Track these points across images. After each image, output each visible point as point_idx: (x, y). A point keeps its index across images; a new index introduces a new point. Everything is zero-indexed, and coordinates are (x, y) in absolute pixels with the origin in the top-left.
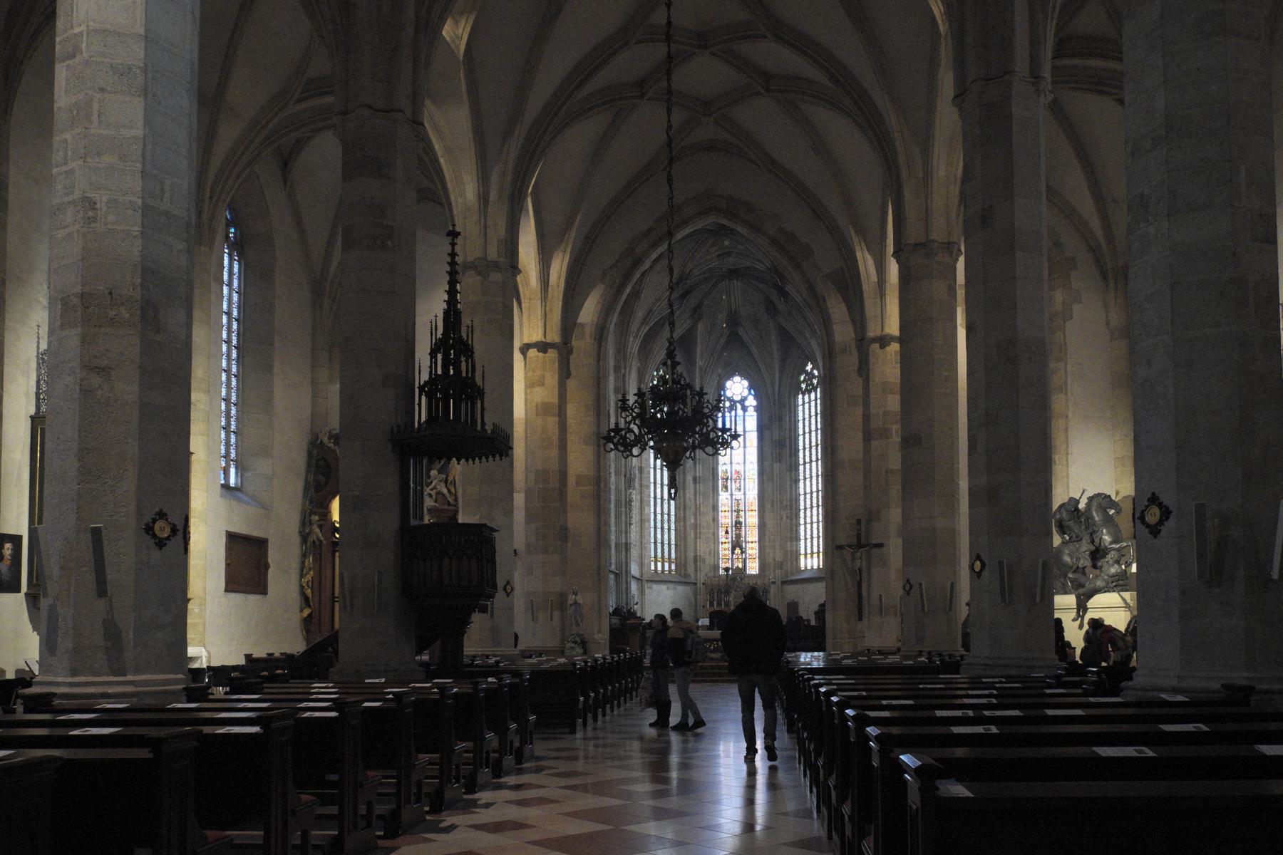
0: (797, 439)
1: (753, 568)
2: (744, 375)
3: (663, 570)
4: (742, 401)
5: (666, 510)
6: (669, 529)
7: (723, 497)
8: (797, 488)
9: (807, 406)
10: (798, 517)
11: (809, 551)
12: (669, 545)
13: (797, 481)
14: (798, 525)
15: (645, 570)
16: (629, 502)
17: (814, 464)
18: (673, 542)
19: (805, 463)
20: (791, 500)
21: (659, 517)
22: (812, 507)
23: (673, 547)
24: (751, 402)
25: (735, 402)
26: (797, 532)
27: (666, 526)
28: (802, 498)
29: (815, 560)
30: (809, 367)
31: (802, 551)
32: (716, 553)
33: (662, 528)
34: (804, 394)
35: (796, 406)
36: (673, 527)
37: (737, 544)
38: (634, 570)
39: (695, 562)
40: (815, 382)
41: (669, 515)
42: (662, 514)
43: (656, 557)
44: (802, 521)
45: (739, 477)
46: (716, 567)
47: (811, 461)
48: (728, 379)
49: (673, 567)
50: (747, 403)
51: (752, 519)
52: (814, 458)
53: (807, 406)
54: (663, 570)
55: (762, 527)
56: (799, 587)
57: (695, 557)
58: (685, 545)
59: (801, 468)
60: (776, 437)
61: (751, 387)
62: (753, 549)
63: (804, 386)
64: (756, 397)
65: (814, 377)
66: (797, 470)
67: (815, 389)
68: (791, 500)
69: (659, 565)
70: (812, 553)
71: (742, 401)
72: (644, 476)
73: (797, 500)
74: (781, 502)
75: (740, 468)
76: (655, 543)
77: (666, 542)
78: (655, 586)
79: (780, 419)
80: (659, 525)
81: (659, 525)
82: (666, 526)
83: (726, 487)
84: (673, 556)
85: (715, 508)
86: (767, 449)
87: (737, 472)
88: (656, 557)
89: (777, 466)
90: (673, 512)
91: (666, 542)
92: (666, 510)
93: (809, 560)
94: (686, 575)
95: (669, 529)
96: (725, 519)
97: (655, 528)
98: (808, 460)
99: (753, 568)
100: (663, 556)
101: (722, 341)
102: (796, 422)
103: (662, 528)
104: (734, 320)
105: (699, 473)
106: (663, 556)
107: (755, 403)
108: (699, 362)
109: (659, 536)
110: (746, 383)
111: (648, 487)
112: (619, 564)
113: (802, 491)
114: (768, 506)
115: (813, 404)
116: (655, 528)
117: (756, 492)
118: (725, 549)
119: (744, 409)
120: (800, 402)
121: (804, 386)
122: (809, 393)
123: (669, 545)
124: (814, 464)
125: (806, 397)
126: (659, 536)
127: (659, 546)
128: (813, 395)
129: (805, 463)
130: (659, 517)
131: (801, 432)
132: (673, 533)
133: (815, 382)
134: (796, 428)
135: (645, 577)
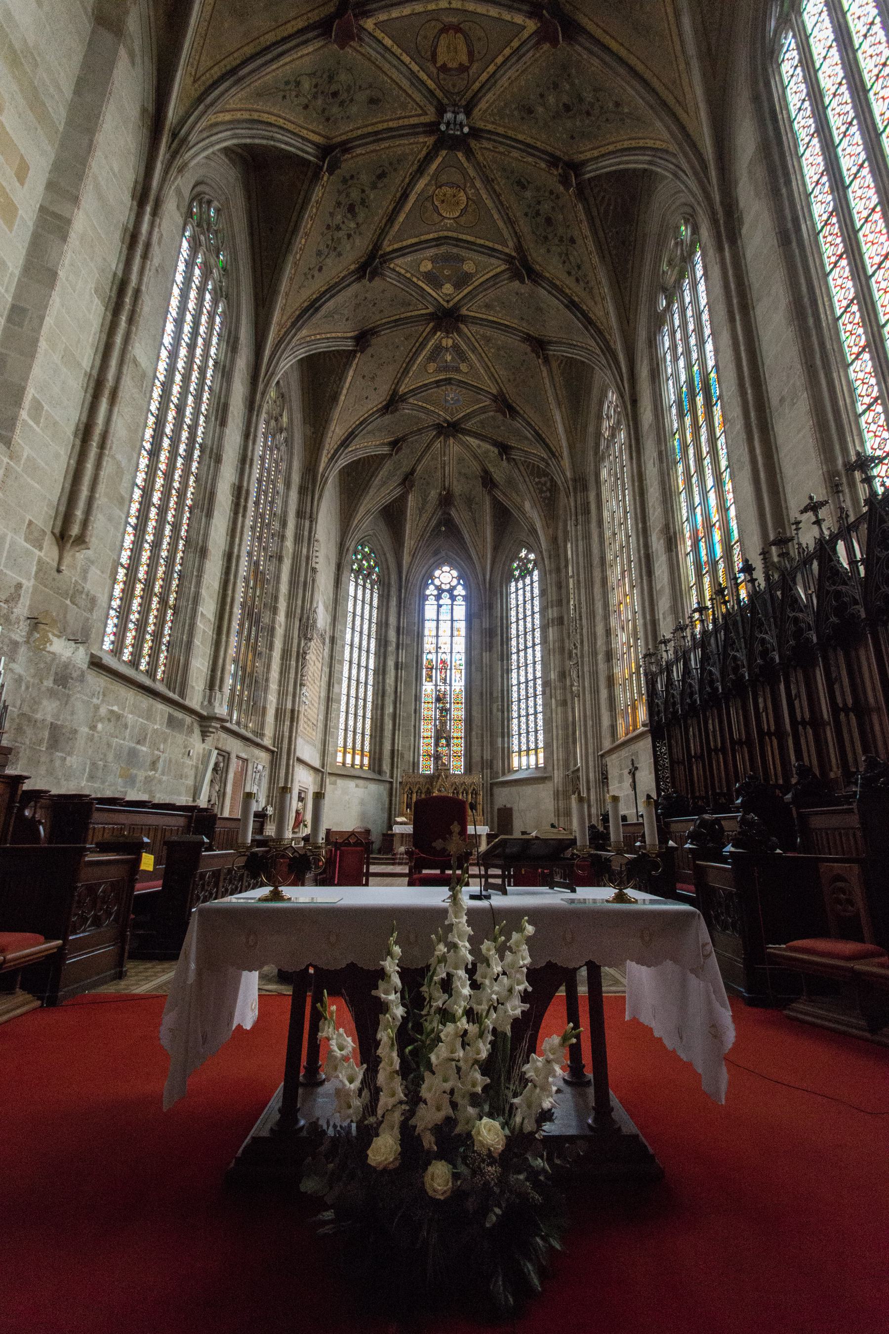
0: (508, 627)
2: (453, 566)
3: (353, 765)
4: (451, 590)
5: (361, 695)
6: (364, 717)
7: (428, 688)
9: (521, 592)
10: (509, 710)
11: (524, 747)
12: (363, 734)
13: (509, 671)
14: (509, 719)
15: (329, 760)
16: (302, 656)
18: (368, 732)
19: (518, 651)
21: (352, 701)
22: (527, 698)
23: (367, 738)
24: (460, 591)
25: (444, 591)
27: (360, 712)
28: (515, 689)
30: (523, 554)
31: (516, 748)
32: (416, 748)
33: (356, 715)
34: (517, 581)
35: (508, 594)
36: (369, 714)
37: (441, 734)
38: (307, 750)
39: (392, 758)
40: (530, 566)
41: (365, 700)
42: (357, 698)
43: (345, 747)
44: (515, 715)
46: (415, 765)
47: (526, 648)
48: (437, 568)
49: (366, 761)
50: (455, 593)
51: (458, 712)
53: (521, 592)
54: (353, 765)
55: (469, 721)
57: (393, 751)
58: (382, 737)
59: (514, 657)
60: (485, 625)
61: (459, 578)
62: (458, 746)
63: (517, 573)
64: (465, 587)
65: (529, 561)
66: (509, 658)
67: (530, 573)
68: (502, 691)
69: (349, 758)
70: (528, 750)
71: (451, 590)
72: (337, 648)
74: (491, 694)
75: (447, 657)
76: (346, 730)
77: (359, 730)
79: (491, 607)
80: (352, 710)
81: (352, 710)
82: (360, 712)
83: (431, 677)
84: (367, 748)
85: (417, 698)
86: (476, 638)
87: (443, 662)
88: (345, 747)
89: (486, 656)
91: (359, 730)
92: (361, 695)
93: (524, 759)
94: (380, 772)
95: (364, 717)
96: (428, 710)
97: (347, 713)
98: (522, 647)
99: (457, 766)
100: (354, 748)
101: (434, 522)
102: (508, 610)
103: (356, 715)
104: (446, 500)
105: (402, 658)
106: (354, 748)
107: (463, 593)
108: (409, 543)
109: (351, 722)
110: (455, 573)
111: (341, 662)
112: (278, 739)
113: (515, 682)
115: (528, 588)
116: (347, 713)
117: (463, 683)
118: (426, 745)
119: (453, 598)
120: (513, 589)
121: (517, 573)
122: (523, 578)
123: (363, 734)
125: (520, 585)
126: (351, 722)
127: (350, 735)
128: (528, 580)
129: (518, 651)
130: (352, 701)
131: (514, 619)
132: (368, 722)
133: (530, 566)
134: (508, 617)
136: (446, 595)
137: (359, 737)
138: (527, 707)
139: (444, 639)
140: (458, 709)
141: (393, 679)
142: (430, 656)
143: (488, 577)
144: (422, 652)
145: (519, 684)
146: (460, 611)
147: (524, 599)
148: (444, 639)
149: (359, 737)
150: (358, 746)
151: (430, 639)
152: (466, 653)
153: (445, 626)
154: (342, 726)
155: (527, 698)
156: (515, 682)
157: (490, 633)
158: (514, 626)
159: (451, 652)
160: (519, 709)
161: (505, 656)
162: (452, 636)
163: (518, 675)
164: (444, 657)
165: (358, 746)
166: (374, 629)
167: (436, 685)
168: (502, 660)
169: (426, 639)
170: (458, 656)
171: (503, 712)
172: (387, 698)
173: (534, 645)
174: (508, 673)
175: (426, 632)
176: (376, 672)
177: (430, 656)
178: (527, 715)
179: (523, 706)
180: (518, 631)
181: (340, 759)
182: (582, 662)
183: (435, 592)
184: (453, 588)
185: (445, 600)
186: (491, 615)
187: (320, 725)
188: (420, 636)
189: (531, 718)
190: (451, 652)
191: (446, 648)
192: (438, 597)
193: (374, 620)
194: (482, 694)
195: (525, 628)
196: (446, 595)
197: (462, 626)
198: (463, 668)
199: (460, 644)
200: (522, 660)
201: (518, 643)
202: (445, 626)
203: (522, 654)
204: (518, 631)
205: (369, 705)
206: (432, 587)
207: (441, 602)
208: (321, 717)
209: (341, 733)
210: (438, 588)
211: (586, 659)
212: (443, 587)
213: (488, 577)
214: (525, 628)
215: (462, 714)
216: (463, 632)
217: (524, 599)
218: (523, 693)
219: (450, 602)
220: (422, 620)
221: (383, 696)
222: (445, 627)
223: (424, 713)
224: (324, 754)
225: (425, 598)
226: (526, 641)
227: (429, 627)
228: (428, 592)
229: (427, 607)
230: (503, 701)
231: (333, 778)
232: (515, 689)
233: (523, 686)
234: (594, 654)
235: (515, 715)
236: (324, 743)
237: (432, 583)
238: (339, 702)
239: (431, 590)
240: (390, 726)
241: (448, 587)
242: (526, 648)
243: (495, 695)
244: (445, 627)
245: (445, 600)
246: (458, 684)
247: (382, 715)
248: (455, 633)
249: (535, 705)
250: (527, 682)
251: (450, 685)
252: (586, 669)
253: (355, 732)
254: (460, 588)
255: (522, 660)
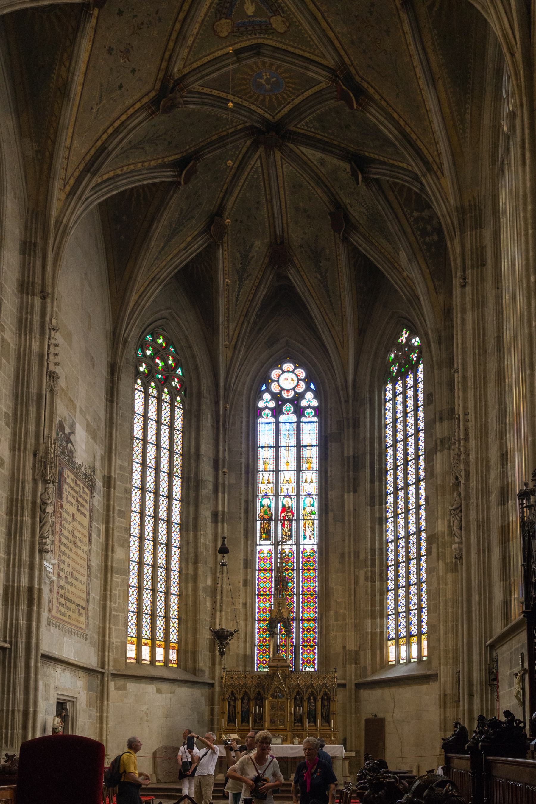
1: (309, 663)
5: (162, 561)
6: (167, 593)
7: (264, 547)
8: (383, 532)
12: (167, 618)
17: (412, 489)
20: (373, 551)
23: (174, 624)
26: (383, 603)
27: (161, 587)
28: (391, 546)
29: (414, 649)
36: (174, 589)
43: (139, 636)
44: (391, 585)
45: (289, 516)
47: (407, 484)
50: (304, 403)
52: (412, 479)
56: (388, 692)
59: (390, 499)
60: (349, 451)
66: (383, 501)
68: (373, 551)
73: (383, 552)
74: (357, 555)
78: (132, 687)
79: (356, 424)
82: (161, 587)
83: (268, 532)
85: (249, 564)
86: (335, 471)
88: (139, 636)
89: (349, 498)
90: (175, 564)
92: (162, 561)
100: (153, 638)
105: (224, 504)
106: (153, 638)
107: (315, 403)
113: (391, 537)
114: (334, 562)
117: (316, 541)
119: (299, 412)
123: (167, 618)
124: (412, 489)
131: (390, 442)
134: (382, 438)
135: (111, 668)
136: (288, 407)
137: (160, 623)
138: (408, 573)
139: (288, 475)
140: (309, 579)
141: (210, 537)
142: (266, 502)
143: (351, 378)
144: (255, 496)
145: (397, 538)
146: (310, 433)
147: (403, 409)
148: (288, 475)
149: (160, 623)
150: (160, 635)
151: (266, 476)
152: (320, 495)
153: (287, 454)
154: (133, 606)
155: (408, 560)
156: (391, 537)
157: (355, 463)
158: (390, 451)
159: (298, 495)
160: (397, 576)
161: (378, 498)
162: (299, 470)
163: (396, 527)
164: (287, 501)
165: (160, 635)
166: (178, 461)
167: (276, 544)
168: (373, 505)
169: (260, 476)
170: (308, 501)
171: (373, 581)
172: (201, 566)
173: (418, 480)
174: (381, 524)
175: (261, 466)
176: (184, 527)
177: (266, 502)
178: (408, 585)
179: (402, 572)
180: (395, 459)
181: (131, 653)
182: (467, 505)
183: (272, 404)
184: (300, 397)
185: (288, 416)
186: (356, 436)
187: (94, 607)
188: (250, 471)
189: (414, 589)
190: (298, 495)
191: (288, 487)
192: (277, 412)
193: (178, 449)
194: (343, 555)
195: (406, 454)
196: (288, 407)
197: (312, 454)
198: (315, 517)
199: (311, 482)
200: (401, 504)
201: (396, 478)
202: (287, 454)
203: (401, 494)
204: (395, 459)
205: (175, 577)
206: (267, 396)
207: (282, 418)
208: (95, 595)
209: (132, 618)
210: (276, 397)
211: (473, 501)
212: (284, 394)
213: (351, 378)
214: (406, 454)
215: (315, 585)
216: (315, 465)
217: (403, 409)
218: (402, 552)
219: (293, 418)
220: (253, 447)
221: (196, 562)
222: (288, 456)
223: (260, 585)
224: (103, 647)
225: (258, 413)
226: (406, 474)
227: (265, 456)
228: (261, 404)
229: (261, 428)
230: (373, 564)
231: (121, 682)
232: (391, 546)
233: (402, 543)
234: (486, 491)
235: (391, 585)
236: (103, 632)
237: (268, 390)
238: (126, 573)
239: (266, 401)
240: (209, 605)
241: (291, 394)
242: (407, 484)
243: (362, 556)
244: (288, 456)
245: (288, 416)
246: (310, 543)
247: (195, 590)
248: (304, 466)
249: (419, 570)
250: (408, 535)
251: (298, 544)
252: (473, 516)
253: (153, 615)
254: (309, 395)
255: (401, 504)
